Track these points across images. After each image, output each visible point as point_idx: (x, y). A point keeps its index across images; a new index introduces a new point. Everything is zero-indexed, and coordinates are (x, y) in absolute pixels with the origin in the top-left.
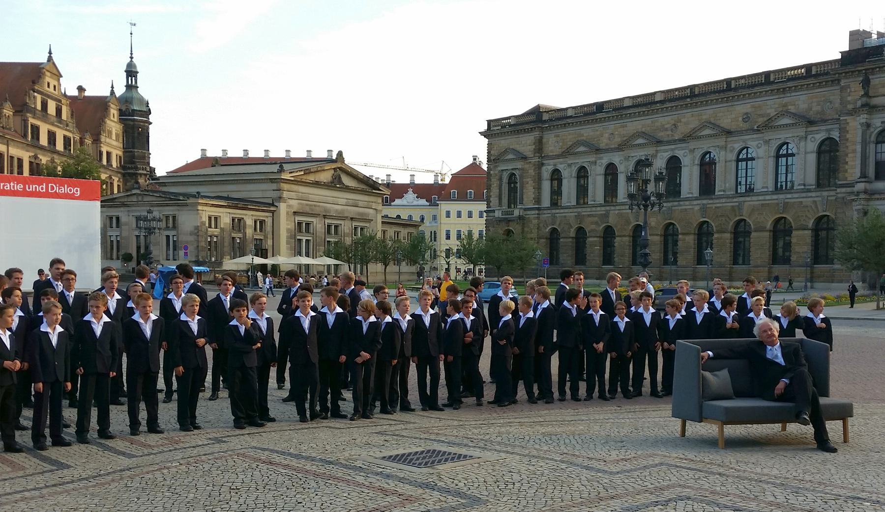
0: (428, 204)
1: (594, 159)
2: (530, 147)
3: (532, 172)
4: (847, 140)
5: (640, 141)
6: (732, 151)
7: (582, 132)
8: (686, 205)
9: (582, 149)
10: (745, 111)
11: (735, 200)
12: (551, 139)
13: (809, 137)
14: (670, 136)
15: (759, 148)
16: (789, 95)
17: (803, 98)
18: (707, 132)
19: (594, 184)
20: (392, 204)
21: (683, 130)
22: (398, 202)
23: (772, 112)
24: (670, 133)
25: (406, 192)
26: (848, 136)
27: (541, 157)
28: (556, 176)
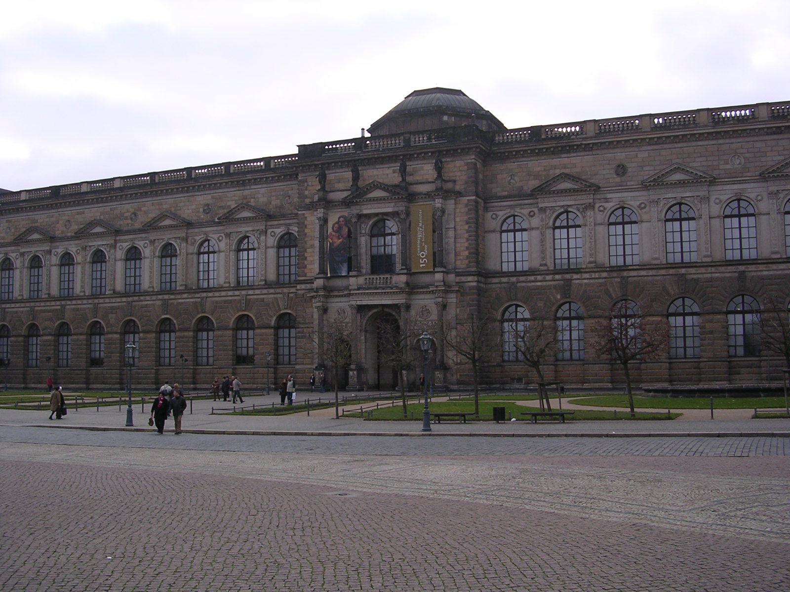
1: (48, 248)
5: (98, 230)
6: (193, 244)
7: (37, 217)
8: (148, 301)
11: (198, 295)
13: (269, 231)
14: (130, 225)
15: (220, 241)
16: (248, 187)
18: (167, 222)
19: (49, 276)
21: (143, 219)
24: (130, 222)
26: (306, 231)
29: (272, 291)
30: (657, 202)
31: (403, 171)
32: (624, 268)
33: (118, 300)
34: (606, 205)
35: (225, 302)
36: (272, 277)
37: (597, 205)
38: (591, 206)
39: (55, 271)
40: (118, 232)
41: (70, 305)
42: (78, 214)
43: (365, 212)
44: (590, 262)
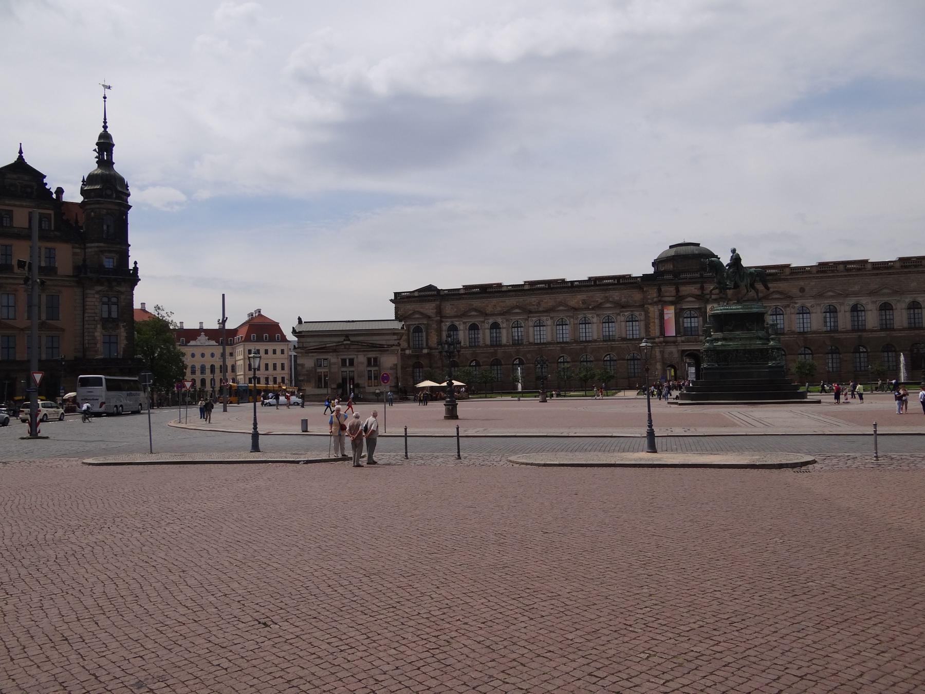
0: (217, 344)
1: (483, 320)
2: (432, 311)
3: (434, 326)
4: (649, 316)
9: (473, 313)
10: (583, 298)
11: (582, 345)
12: (447, 307)
13: (621, 314)
17: (617, 294)
18: (561, 308)
20: (189, 344)
22: (192, 343)
23: (600, 301)
24: (536, 307)
25: (200, 335)
26: (649, 315)
27: (441, 317)
28: (453, 328)
29: (625, 342)
30: (819, 305)
31: (702, 288)
32: (804, 333)
33: (532, 347)
34: (795, 305)
35: (599, 348)
36: (624, 336)
37: (791, 305)
38: (788, 306)
39: (488, 332)
40: (530, 312)
41: (500, 350)
42: (502, 302)
43: (684, 307)
44: (788, 331)
